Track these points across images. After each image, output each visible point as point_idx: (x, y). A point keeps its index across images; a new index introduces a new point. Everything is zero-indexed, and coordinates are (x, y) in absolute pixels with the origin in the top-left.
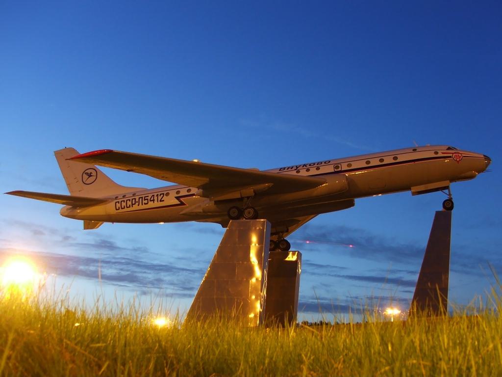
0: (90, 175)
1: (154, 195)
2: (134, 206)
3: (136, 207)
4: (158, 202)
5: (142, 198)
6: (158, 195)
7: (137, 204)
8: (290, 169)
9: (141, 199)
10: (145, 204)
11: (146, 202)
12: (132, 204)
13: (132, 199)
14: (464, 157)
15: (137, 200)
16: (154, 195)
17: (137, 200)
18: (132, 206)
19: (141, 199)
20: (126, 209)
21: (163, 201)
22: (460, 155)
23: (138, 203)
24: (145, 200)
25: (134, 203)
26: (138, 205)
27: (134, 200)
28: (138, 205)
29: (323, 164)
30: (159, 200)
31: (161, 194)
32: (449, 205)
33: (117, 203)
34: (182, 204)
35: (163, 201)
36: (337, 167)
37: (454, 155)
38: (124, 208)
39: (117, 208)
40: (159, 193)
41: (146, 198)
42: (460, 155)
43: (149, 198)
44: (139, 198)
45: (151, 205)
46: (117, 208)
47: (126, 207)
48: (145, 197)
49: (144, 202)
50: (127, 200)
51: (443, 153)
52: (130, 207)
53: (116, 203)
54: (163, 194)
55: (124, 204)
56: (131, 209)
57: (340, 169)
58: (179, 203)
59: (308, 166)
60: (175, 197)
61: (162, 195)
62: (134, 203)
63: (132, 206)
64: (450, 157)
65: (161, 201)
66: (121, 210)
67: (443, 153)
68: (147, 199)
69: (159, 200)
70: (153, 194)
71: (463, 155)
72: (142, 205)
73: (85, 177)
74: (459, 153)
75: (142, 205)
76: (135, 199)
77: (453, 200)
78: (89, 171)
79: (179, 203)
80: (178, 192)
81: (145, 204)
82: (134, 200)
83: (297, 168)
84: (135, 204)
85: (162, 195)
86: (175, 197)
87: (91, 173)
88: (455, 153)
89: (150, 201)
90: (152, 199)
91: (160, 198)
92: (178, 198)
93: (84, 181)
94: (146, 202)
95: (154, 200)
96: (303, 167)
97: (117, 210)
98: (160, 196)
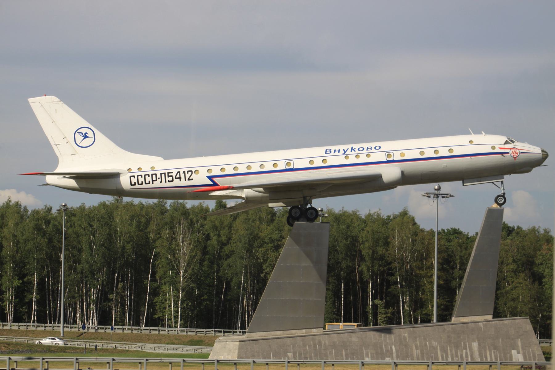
0: (85, 136)
1: (179, 172)
2: (154, 182)
3: (157, 184)
4: (185, 180)
5: (165, 174)
6: (184, 172)
7: (159, 180)
8: (337, 153)
9: (163, 175)
10: (169, 181)
11: (170, 179)
12: (153, 181)
13: (152, 175)
14: (521, 153)
15: (159, 176)
16: (179, 172)
17: (159, 176)
18: (153, 183)
19: (163, 175)
20: (144, 186)
21: (192, 179)
22: (517, 151)
23: (159, 180)
24: (169, 176)
25: (154, 179)
26: (161, 182)
27: (154, 176)
28: (161, 182)
29: (373, 150)
30: (187, 179)
31: (188, 172)
32: (501, 199)
33: (132, 178)
34: (215, 184)
35: (192, 179)
36: (388, 155)
37: (512, 150)
38: (142, 184)
39: (133, 183)
40: (186, 170)
41: (170, 175)
42: (517, 151)
43: (174, 175)
44: (161, 174)
45: (176, 183)
46: (133, 183)
47: (144, 183)
48: (168, 173)
49: (168, 179)
50: (145, 175)
51: (501, 148)
52: (149, 183)
53: (131, 177)
54: (192, 171)
55: (141, 180)
56: (151, 185)
57: (392, 159)
58: (212, 183)
59: (357, 152)
60: (208, 177)
61: (190, 173)
62: (154, 179)
63: (153, 183)
64: (508, 153)
65: (189, 179)
66: (137, 186)
67: (501, 148)
68: (172, 176)
69: (187, 179)
70: (179, 170)
71: (521, 151)
72: (166, 182)
73: (79, 138)
74: (517, 149)
75: (166, 182)
76: (156, 174)
77: (506, 196)
78: (84, 131)
79: (212, 183)
80: (209, 170)
81: (169, 181)
82: (154, 176)
83: (345, 152)
84: (156, 180)
85: (190, 173)
86: (208, 177)
87: (86, 133)
88: (512, 149)
89: (176, 178)
90: (178, 176)
91: (188, 176)
92: (210, 178)
93: (78, 144)
94: (170, 179)
95: (180, 178)
96: (351, 151)
97: (131, 185)
98: (188, 173)
